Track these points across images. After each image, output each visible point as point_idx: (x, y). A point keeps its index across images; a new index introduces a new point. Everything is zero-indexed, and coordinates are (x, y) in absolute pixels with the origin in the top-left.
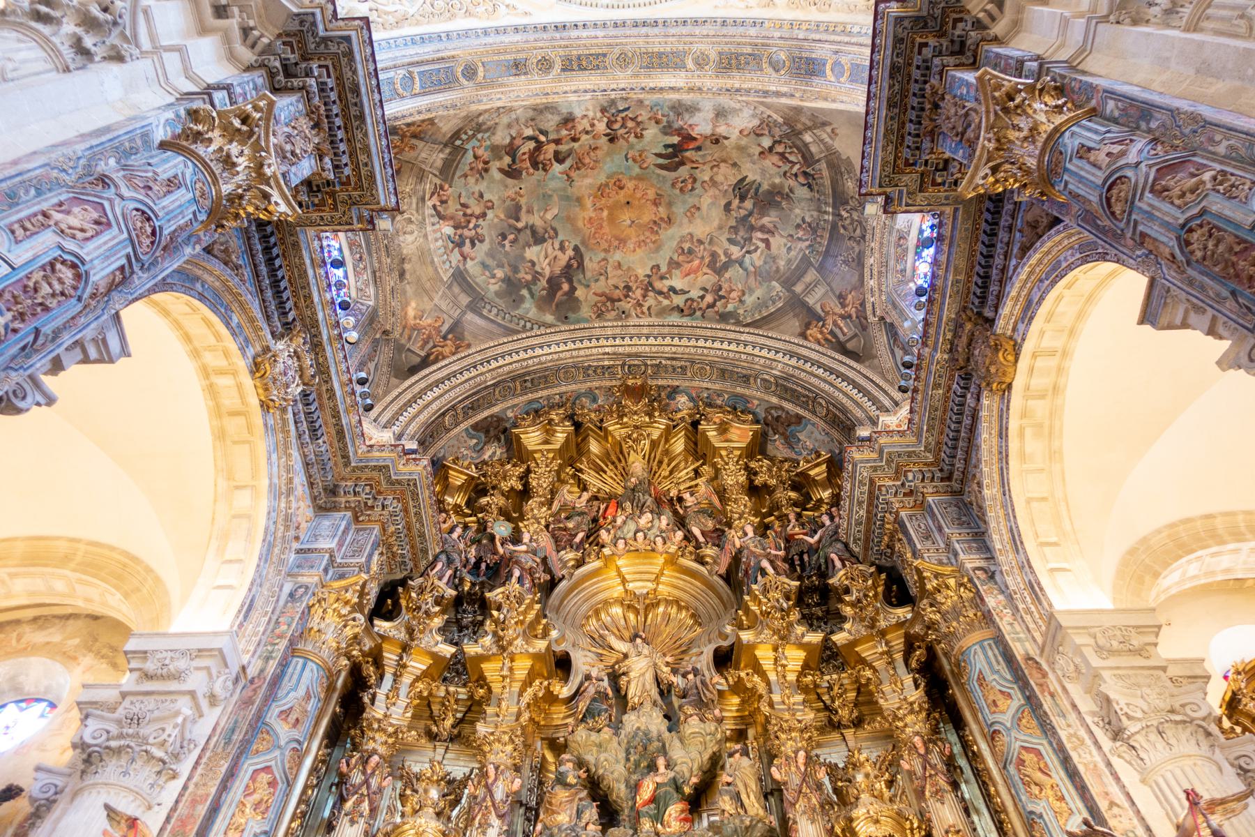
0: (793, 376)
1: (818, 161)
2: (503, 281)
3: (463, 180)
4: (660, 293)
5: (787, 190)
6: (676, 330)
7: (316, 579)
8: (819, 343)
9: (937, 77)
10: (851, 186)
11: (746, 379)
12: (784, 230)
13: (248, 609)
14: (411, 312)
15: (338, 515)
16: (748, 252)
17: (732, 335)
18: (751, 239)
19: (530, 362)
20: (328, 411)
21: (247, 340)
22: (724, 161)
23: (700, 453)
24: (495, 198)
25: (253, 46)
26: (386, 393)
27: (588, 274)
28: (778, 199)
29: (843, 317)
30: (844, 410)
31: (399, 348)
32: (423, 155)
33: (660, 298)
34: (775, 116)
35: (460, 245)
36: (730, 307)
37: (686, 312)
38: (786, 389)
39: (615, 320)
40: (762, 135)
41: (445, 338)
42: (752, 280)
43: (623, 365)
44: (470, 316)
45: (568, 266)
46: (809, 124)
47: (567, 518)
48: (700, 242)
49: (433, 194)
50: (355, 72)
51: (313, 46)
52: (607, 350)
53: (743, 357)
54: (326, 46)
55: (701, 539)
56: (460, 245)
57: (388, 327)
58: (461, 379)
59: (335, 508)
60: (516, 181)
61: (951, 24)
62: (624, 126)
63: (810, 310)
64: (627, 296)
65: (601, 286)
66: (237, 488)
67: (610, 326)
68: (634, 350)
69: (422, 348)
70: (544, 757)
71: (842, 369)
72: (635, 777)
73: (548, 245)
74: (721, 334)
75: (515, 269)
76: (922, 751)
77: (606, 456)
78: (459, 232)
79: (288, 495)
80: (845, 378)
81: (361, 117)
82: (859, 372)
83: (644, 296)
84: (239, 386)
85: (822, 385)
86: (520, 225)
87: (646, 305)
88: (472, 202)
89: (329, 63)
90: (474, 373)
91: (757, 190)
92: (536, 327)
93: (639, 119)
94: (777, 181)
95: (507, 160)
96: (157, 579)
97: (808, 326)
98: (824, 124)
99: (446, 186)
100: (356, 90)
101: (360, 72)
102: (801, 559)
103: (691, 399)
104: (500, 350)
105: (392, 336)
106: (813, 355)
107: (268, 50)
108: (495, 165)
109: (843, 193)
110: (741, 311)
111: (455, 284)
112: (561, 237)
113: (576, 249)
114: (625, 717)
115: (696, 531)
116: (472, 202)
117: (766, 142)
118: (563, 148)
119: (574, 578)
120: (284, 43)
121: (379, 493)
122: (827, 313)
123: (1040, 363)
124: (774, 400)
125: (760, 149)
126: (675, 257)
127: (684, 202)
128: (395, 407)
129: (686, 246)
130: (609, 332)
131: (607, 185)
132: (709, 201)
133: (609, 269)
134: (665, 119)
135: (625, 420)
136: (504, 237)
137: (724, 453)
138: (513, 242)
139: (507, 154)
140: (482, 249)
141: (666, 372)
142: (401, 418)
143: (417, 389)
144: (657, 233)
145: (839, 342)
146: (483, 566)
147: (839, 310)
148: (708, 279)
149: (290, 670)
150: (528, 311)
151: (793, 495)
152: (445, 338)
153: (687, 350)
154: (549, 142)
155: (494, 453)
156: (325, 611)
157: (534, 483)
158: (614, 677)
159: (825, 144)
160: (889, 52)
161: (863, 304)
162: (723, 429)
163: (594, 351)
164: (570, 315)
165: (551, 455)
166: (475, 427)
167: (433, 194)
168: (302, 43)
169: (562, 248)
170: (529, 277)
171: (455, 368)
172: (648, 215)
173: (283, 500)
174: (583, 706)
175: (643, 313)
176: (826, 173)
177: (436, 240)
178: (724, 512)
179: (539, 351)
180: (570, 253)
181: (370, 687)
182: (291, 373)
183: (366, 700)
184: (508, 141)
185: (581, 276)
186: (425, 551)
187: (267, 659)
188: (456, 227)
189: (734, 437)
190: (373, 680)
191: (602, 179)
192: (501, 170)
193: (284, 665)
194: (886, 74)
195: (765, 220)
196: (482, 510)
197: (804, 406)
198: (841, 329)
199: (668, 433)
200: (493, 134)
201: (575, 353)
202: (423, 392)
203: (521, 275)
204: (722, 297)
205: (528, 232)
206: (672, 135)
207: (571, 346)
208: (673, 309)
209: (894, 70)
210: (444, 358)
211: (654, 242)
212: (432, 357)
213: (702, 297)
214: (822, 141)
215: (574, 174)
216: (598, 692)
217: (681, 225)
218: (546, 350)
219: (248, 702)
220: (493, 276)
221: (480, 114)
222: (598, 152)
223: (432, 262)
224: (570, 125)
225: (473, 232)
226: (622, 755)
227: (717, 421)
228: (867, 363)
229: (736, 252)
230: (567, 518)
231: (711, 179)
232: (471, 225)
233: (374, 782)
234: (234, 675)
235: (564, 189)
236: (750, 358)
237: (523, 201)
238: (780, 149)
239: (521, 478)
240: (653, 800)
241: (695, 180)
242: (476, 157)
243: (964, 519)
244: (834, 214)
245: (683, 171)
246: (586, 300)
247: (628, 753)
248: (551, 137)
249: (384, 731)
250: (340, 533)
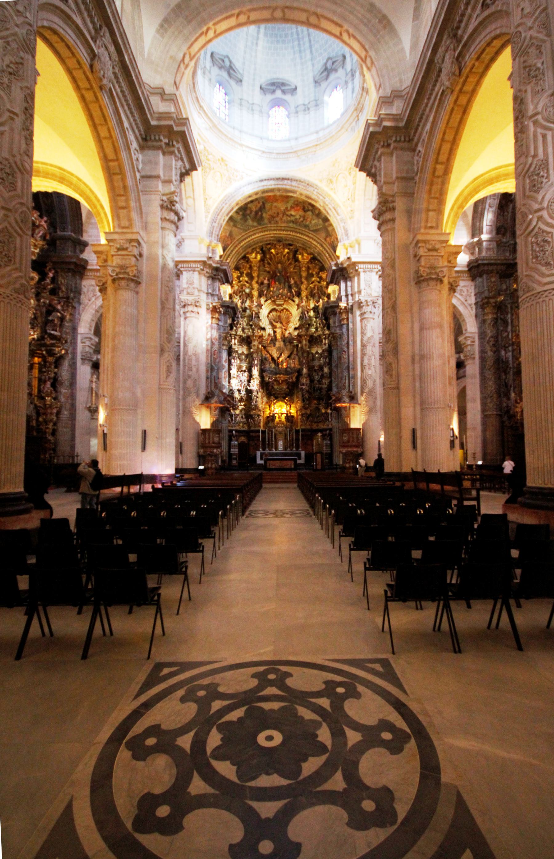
4: (287, 215)
36: (307, 223)
44: (234, 229)
65: (270, 213)
77: (271, 259)
90: (237, 249)
97: (327, 236)
130: (273, 228)
151: (318, 279)
162: (303, 256)
164: (262, 223)
169: (259, 203)
180: (261, 203)
207: (262, 234)
229: (310, 208)
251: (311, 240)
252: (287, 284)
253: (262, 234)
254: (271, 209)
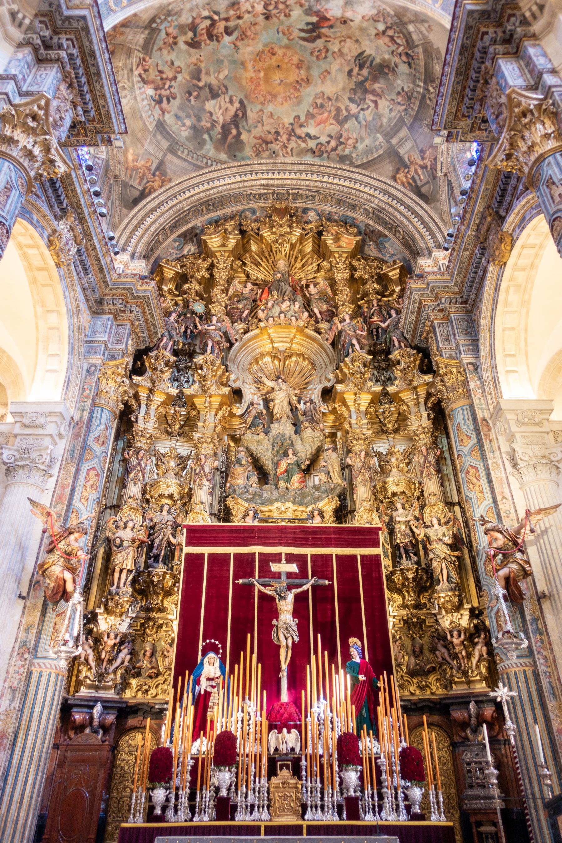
0: (384, 209)
1: (417, 46)
2: (191, 128)
3: (159, 52)
4: (300, 138)
5: (393, 65)
6: (309, 168)
7: (100, 361)
8: (404, 186)
9: (490, 61)
10: (438, 68)
11: (354, 207)
12: (389, 95)
13: (68, 383)
14: (130, 157)
16: (362, 109)
17: (347, 174)
18: (364, 99)
19: (212, 192)
20: (93, 257)
21: (43, 228)
22: (350, 37)
23: (321, 253)
24: (182, 65)
25: (20, 25)
26: (121, 221)
27: (250, 122)
28: (386, 71)
29: (422, 167)
30: (414, 240)
31: (125, 185)
32: (130, 37)
33: (300, 142)
34: (389, 10)
35: (160, 102)
36: (347, 152)
37: (317, 154)
38: (379, 217)
39: (269, 158)
40: (378, 21)
41: (154, 175)
42: (363, 132)
43: (273, 193)
44: (169, 157)
45: (236, 115)
46: (412, 18)
47: (238, 301)
48: (329, 99)
49: (138, 65)
50: (91, 42)
51: (60, 22)
52: (263, 182)
53: (353, 191)
54: (70, 23)
55: (319, 316)
56: (160, 102)
57: (117, 173)
58: (167, 206)
59: (102, 313)
60: (197, 51)
61: (506, 18)
62: (276, 7)
63: (400, 159)
64: (276, 140)
65: (258, 131)
66: (48, 311)
67: (265, 163)
68: (281, 182)
69: (140, 183)
70: (229, 445)
71: (416, 208)
72: (277, 458)
73: (221, 99)
74: (339, 172)
75: (199, 119)
76: (425, 454)
77: (261, 254)
78: (158, 92)
79: (78, 314)
80: (417, 215)
81: (98, 74)
82: (426, 212)
83: (289, 140)
84: (42, 254)
85: (402, 219)
86: (201, 84)
87: (290, 147)
88: (166, 69)
89: (72, 37)
90: (175, 201)
91: (372, 62)
92: (214, 163)
93: (288, 3)
94: (387, 57)
95: (190, 34)
96: (9, 358)
97: (397, 171)
98: (423, 21)
99: (147, 58)
100: (93, 55)
101: (95, 41)
102: (377, 332)
103: (318, 214)
104: (191, 183)
105: (120, 179)
106: (399, 195)
107: (30, 28)
108: (181, 39)
109: (432, 73)
110: (354, 155)
111: (158, 132)
112: (230, 93)
113: (241, 102)
114: (272, 426)
115: (316, 311)
116: (166, 69)
117: (381, 27)
118: (231, 24)
119: (243, 341)
120: (41, 22)
121: (127, 303)
122: (411, 163)
123: (525, 251)
124: (371, 223)
125: (375, 32)
126: (311, 110)
127: (319, 67)
128: (127, 232)
129: (319, 101)
130: (264, 167)
131: (263, 52)
132: (337, 67)
133: (265, 118)
134: (307, 4)
135: (274, 230)
136: (190, 94)
137: (336, 255)
138: (197, 97)
139: (190, 30)
140: (175, 103)
141: (302, 198)
142: (132, 241)
143: (139, 217)
144: (299, 90)
145: (417, 186)
146: (189, 331)
147: (420, 162)
148: (333, 128)
149: (95, 415)
150: (209, 151)
151: (377, 287)
152: (154, 175)
153: (316, 184)
154: (220, 20)
155: (190, 250)
156: (107, 380)
157: (217, 276)
158: (267, 402)
159: (423, 35)
160: (461, 35)
161: (435, 159)
162: (337, 239)
163: (254, 183)
164: (238, 154)
165: (227, 254)
166: (179, 236)
167: (138, 65)
168: (53, 21)
169: (231, 102)
170: (208, 125)
171: (162, 198)
172: (292, 77)
173: (75, 317)
174: (249, 421)
175: (287, 153)
176: (421, 56)
177: (143, 100)
178: (333, 299)
179: (217, 183)
180: (237, 105)
181: (134, 411)
182: (70, 242)
183: (133, 419)
184: (190, 20)
185: (245, 123)
186: (157, 333)
187: (83, 410)
188: (156, 89)
189: (344, 244)
190: (135, 407)
191: (260, 47)
192: (186, 43)
193: (91, 412)
194: (458, 51)
195: (376, 86)
196: (186, 293)
197: (390, 230)
198: (419, 176)
199: (302, 239)
200: (180, 16)
201: (241, 184)
202: (144, 219)
203: (203, 123)
204: (342, 143)
205: (207, 89)
206: (311, 15)
207: (238, 179)
208: (308, 151)
209: (463, 49)
210: (155, 190)
211: (297, 98)
212: (147, 191)
213: (328, 142)
214: (421, 32)
215: (239, 44)
216: (257, 413)
217: (316, 85)
218: (222, 182)
219: (77, 435)
220: (184, 125)
221: (170, 4)
222: (257, 27)
223: (141, 117)
224: (236, 7)
225: (168, 92)
226: (270, 447)
227: (334, 232)
228: (432, 205)
229: (354, 108)
230: (238, 301)
231: (340, 50)
232: (167, 87)
233: (143, 463)
235: (232, 55)
236: (357, 193)
237: (202, 65)
238: (390, 33)
239: (208, 269)
240: (286, 471)
241: (327, 51)
242: (167, 34)
243: (469, 330)
244: (424, 88)
245: (319, 43)
246: (248, 142)
247: (273, 446)
248: (223, 16)
249: (145, 437)
251: (357, 186)
252: (300, 298)
253: (238, 179)
254: (260, 121)
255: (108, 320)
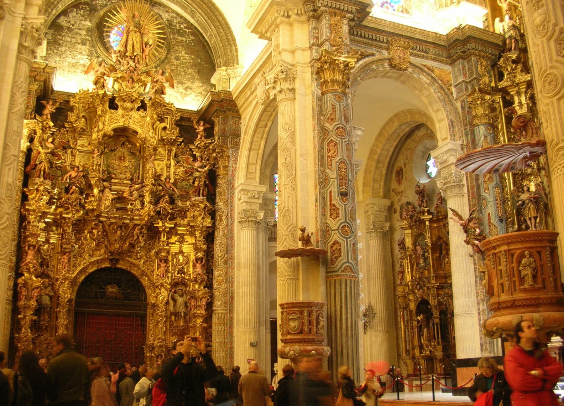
15: (457, 63)
59: (455, 61)
120: (307, 5)
234: (460, 149)
250: (462, 72)
255: (459, 64)
